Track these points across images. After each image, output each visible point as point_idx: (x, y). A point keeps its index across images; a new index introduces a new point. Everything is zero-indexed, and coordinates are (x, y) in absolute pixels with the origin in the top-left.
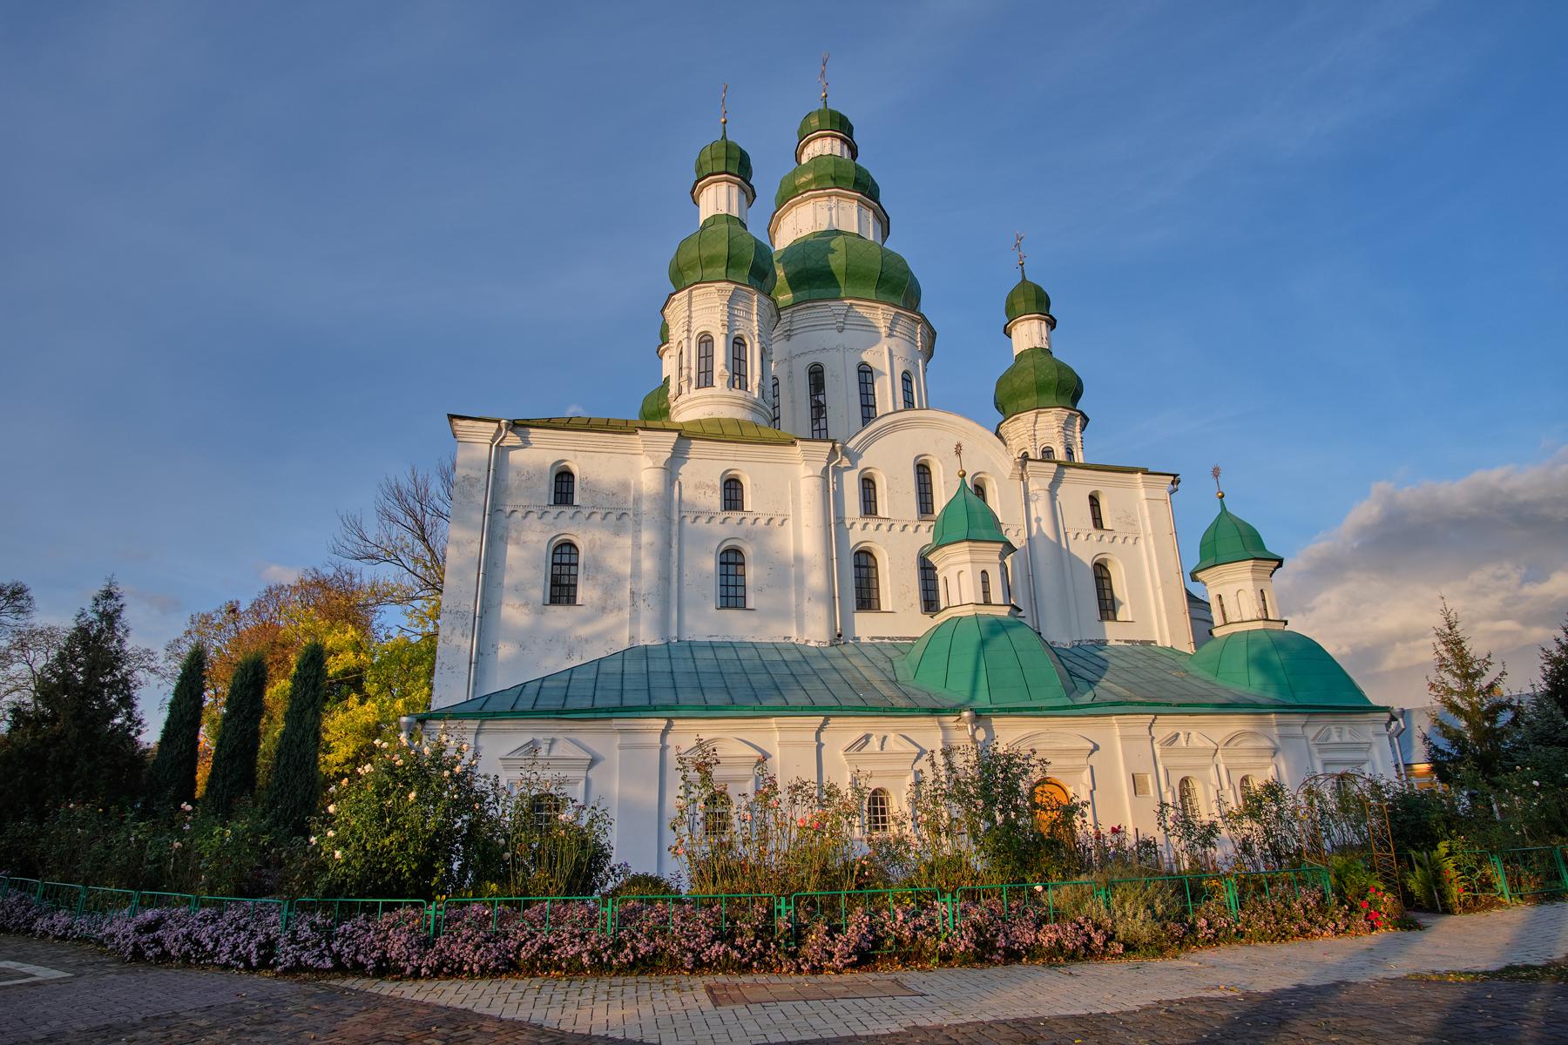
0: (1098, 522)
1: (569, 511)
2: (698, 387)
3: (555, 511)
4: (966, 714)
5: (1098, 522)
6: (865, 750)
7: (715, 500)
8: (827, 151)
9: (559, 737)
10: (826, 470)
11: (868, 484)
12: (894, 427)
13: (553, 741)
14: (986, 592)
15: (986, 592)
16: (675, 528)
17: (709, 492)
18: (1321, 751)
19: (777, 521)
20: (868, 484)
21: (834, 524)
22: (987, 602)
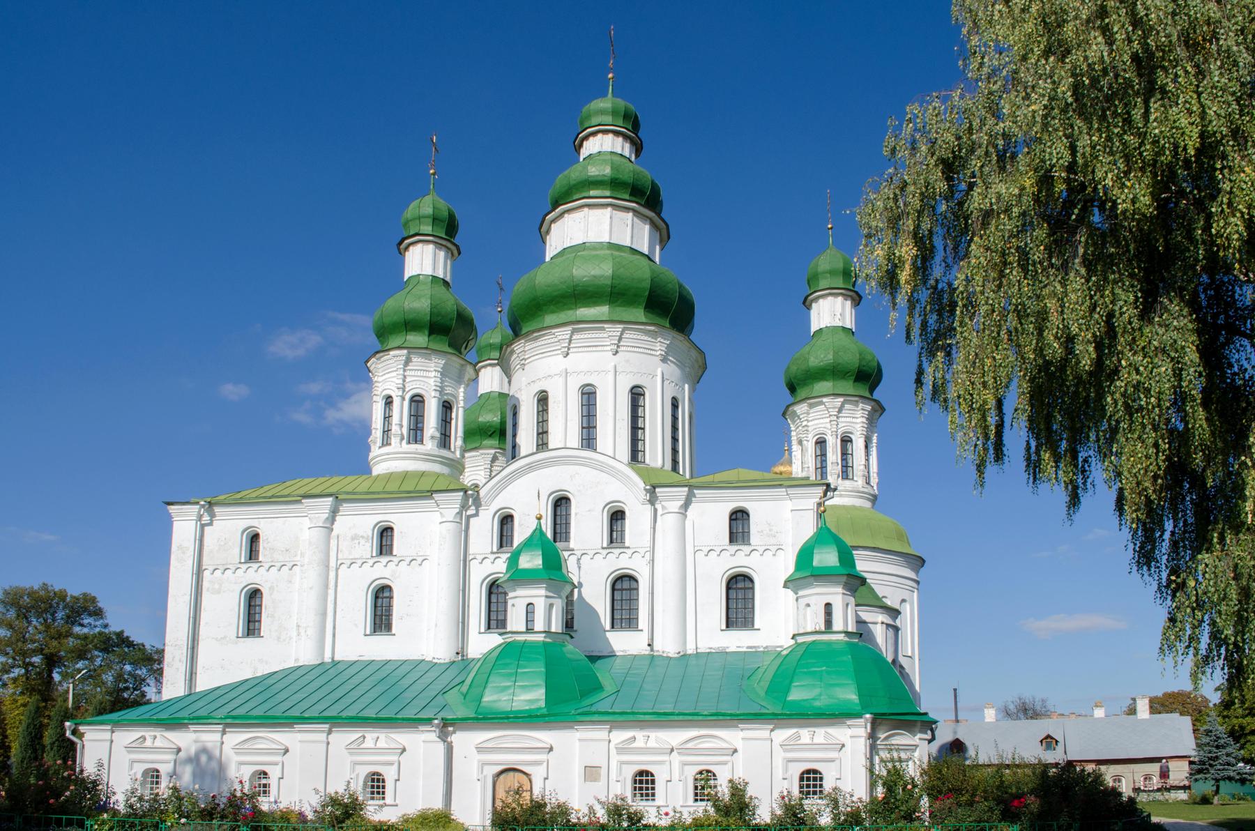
1: (255, 566)
2: (383, 445)
3: (244, 566)
6: (363, 746)
7: (368, 547)
9: (158, 734)
10: (460, 513)
11: (506, 520)
12: (530, 468)
13: (155, 737)
14: (529, 618)
16: (332, 575)
17: (362, 541)
19: (419, 560)
20: (506, 520)
21: (464, 561)
22: (529, 630)
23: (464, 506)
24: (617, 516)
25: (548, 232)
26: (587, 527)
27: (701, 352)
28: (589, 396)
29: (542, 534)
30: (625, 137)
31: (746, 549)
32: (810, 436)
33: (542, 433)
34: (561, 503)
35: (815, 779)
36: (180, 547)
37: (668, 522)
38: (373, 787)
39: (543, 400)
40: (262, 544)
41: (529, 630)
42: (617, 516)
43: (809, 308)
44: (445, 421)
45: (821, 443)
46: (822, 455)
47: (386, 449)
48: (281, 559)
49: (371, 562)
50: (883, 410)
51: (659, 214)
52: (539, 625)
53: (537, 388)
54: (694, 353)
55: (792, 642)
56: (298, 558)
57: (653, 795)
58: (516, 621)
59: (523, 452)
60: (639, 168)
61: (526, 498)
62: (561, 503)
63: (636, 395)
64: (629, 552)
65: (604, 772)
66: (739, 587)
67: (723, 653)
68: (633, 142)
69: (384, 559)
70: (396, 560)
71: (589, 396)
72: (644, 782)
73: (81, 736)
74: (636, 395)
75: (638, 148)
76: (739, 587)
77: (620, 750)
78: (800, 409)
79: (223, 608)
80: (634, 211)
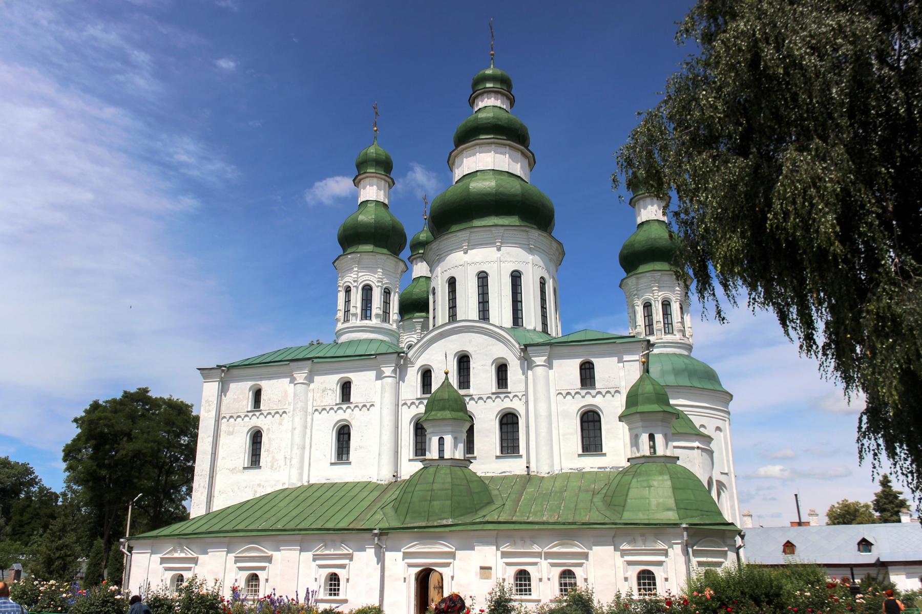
1: (258, 414)
3: (250, 414)
4: (376, 531)
11: (426, 375)
12: (442, 336)
14: (441, 450)
15: (441, 450)
17: (330, 392)
20: (426, 375)
22: (441, 457)
23: (398, 366)
24: (502, 370)
25: (453, 164)
26: (482, 377)
27: (560, 244)
28: (483, 279)
29: (450, 385)
30: (503, 94)
31: (593, 392)
32: (639, 303)
33: (453, 307)
34: (464, 361)
35: (649, 579)
36: (207, 401)
38: (331, 585)
39: (452, 282)
40: (264, 397)
41: (441, 457)
42: (502, 370)
43: (634, 207)
44: (386, 303)
45: (647, 306)
47: (346, 325)
48: (275, 407)
49: (335, 408)
51: (527, 147)
53: (447, 276)
54: (555, 245)
55: (629, 464)
56: (286, 407)
57: (530, 590)
58: (433, 453)
59: (440, 322)
60: (512, 116)
61: (440, 358)
62: (464, 361)
63: (516, 277)
65: (493, 571)
66: (590, 422)
67: (581, 474)
68: (508, 98)
69: (344, 407)
70: (352, 406)
71: (483, 279)
72: (523, 577)
73: (130, 549)
74: (516, 277)
75: (512, 103)
76: (590, 422)
78: (632, 281)
79: (235, 445)
80: (510, 146)
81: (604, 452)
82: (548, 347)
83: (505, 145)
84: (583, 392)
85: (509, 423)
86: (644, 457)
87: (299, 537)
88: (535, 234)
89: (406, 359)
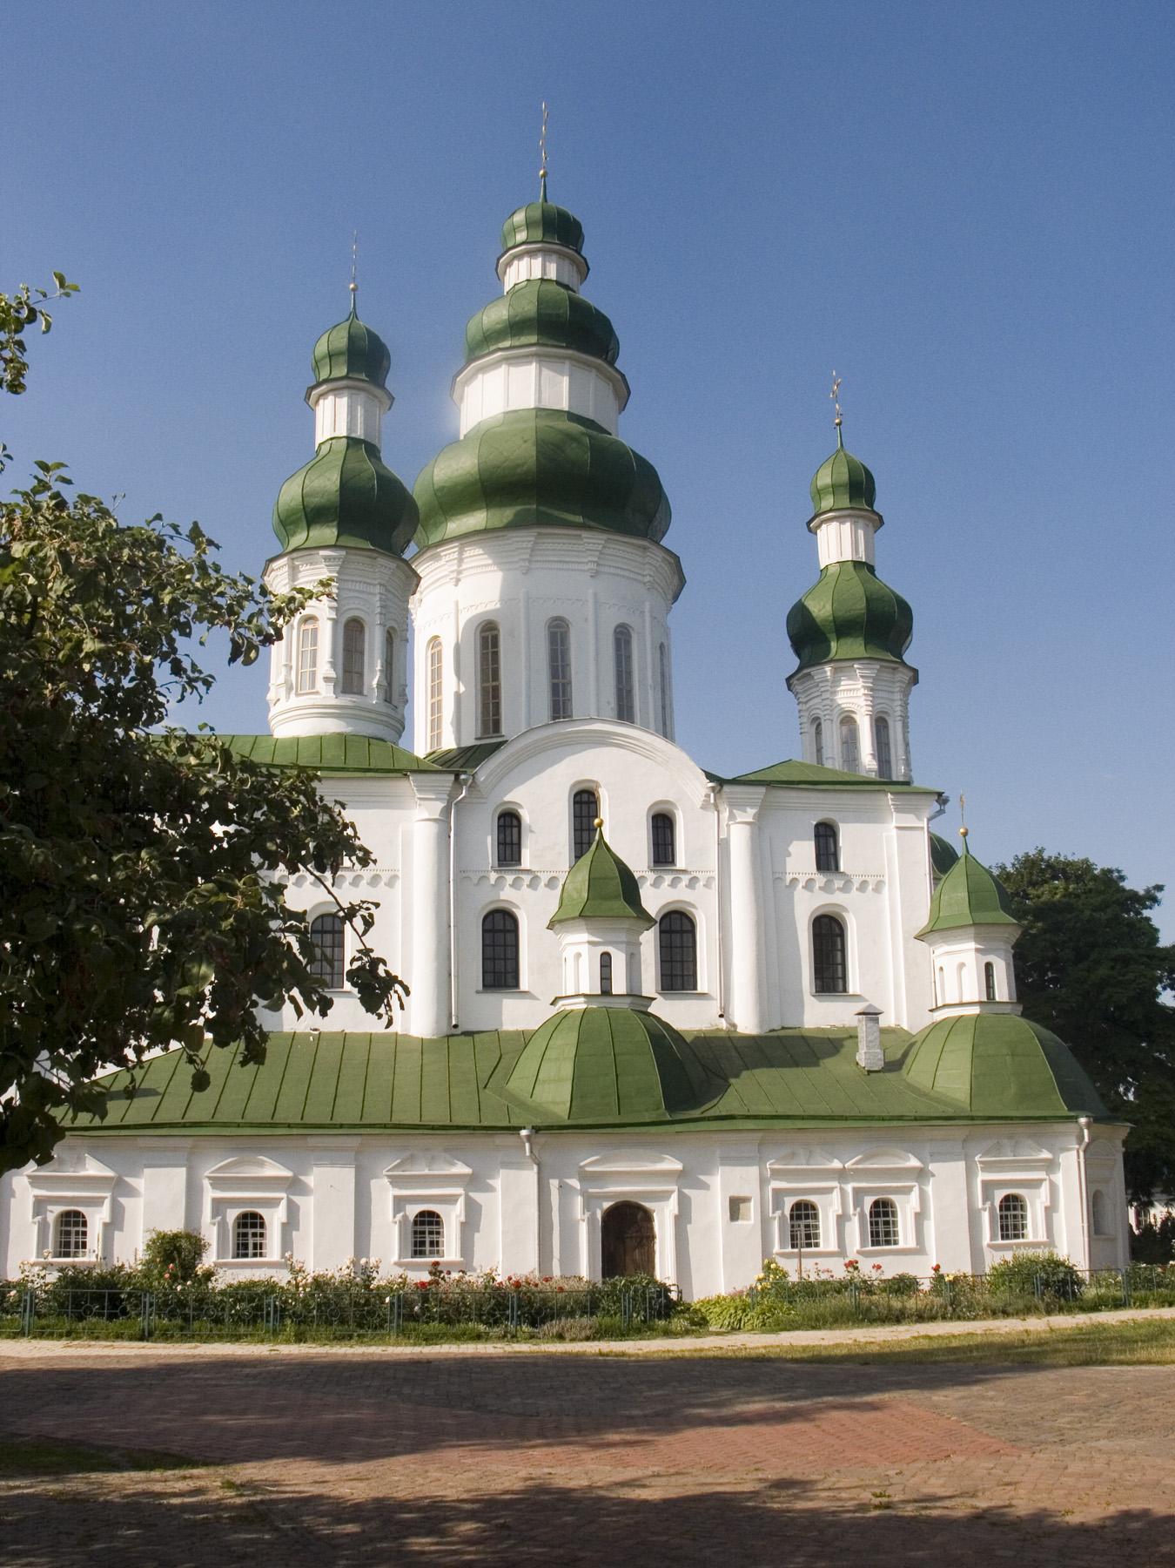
0: (827, 858)
4: (524, 1133)
5: (827, 858)
8: (537, 274)
10: (446, 811)
11: (509, 824)
14: (606, 978)
15: (606, 978)
18: (983, 1170)
22: (606, 992)
24: (662, 825)
26: (626, 838)
28: (558, 634)
31: (838, 883)
34: (585, 803)
37: (739, 838)
41: (606, 992)
42: (662, 825)
43: (813, 531)
46: (851, 742)
50: (915, 680)
52: (619, 987)
54: (676, 581)
62: (585, 803)
64: (685, 879)
68: (579, 272)
71: (558, 634)
74: (622, 637)
77: (776, 1174)
80: (598, 369)
81: (851, 990)
82: (763, 790)
83: (588, 365)
84: (820, 879)
85: (677, 930)
86: (980, 1003)
87: (359, 1139)
88: (655, 556)
89: (473, 786)
